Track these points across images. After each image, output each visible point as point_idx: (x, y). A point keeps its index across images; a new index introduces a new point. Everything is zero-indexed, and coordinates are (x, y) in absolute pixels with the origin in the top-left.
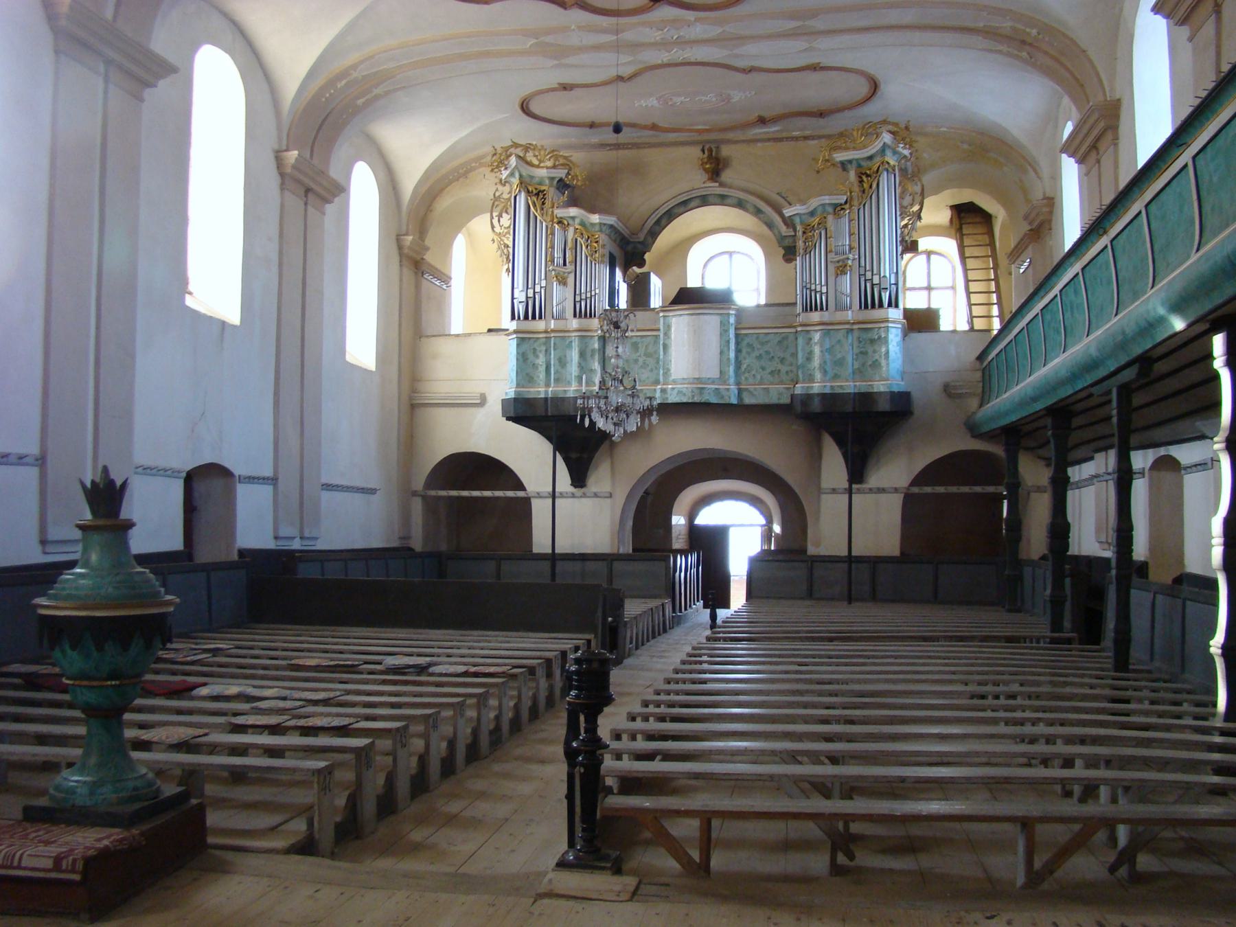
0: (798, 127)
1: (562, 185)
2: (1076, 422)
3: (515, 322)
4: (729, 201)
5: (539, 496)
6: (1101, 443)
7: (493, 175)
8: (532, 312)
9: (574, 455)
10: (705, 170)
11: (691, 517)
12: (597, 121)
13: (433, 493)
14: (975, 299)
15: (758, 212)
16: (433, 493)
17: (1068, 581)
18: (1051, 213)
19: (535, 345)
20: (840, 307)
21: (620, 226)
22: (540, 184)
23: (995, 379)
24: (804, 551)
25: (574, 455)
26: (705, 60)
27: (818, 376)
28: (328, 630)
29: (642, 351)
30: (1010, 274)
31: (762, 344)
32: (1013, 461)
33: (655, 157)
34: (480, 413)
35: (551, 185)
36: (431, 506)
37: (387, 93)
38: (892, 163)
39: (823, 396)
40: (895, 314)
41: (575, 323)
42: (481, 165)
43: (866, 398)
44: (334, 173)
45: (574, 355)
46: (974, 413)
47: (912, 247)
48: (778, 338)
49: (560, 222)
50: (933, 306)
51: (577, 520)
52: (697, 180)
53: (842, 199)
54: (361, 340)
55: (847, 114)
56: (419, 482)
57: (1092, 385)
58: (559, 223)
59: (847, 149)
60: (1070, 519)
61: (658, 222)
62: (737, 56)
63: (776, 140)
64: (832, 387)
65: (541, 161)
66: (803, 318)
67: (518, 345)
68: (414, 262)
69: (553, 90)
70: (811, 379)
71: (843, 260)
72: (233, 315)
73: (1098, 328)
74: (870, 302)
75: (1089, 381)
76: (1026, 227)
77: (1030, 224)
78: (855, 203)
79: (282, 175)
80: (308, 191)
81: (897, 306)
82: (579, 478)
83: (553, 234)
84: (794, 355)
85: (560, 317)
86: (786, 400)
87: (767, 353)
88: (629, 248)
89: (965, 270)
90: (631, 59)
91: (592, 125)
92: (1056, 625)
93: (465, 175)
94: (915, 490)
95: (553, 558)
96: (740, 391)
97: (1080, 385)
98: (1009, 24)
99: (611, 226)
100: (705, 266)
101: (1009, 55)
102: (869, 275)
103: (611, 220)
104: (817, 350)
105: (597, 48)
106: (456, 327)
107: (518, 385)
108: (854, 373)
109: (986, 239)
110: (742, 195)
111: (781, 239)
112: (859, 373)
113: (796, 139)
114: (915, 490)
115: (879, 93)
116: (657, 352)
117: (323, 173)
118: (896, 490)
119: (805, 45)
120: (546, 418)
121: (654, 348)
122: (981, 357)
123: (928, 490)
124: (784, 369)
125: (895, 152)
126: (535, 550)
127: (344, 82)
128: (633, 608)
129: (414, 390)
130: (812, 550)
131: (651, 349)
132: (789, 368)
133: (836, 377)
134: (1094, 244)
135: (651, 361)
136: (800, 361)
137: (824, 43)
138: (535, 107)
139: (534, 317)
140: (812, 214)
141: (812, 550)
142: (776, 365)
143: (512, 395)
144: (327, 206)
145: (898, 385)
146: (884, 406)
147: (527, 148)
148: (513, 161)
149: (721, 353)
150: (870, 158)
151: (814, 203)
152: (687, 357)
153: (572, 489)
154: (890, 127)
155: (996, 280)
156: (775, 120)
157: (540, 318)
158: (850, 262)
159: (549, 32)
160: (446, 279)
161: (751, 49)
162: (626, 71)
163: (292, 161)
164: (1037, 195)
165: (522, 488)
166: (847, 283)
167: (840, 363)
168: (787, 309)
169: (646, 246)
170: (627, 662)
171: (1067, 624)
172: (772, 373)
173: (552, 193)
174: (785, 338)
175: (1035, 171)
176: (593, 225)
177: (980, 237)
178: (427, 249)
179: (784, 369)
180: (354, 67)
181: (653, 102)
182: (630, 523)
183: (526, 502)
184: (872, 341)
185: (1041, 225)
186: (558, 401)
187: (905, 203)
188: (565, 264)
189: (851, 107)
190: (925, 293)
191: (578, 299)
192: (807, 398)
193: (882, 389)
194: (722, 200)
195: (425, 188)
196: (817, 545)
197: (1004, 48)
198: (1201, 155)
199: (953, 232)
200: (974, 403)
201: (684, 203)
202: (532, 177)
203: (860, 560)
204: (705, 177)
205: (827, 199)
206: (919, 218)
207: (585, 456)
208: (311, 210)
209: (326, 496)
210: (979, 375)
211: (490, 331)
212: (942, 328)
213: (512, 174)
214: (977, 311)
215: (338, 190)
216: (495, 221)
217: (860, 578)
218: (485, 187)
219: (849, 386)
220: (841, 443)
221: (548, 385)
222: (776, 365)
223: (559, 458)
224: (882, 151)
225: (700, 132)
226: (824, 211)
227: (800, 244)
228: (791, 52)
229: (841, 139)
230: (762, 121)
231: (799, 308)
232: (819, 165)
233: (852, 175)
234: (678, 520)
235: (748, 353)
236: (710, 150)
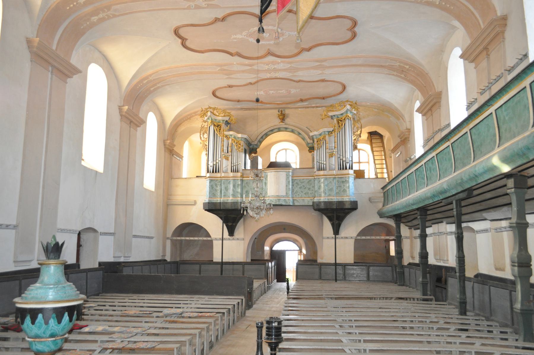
0: (314, 103)
1: (227, 123)
2: (429, 212)
4: (288, 130)
5: (216, 239)
6: (434, 221)
7: (201, 119)
8: (216, 170)
9: (230, 224)
10: (280, 118)
11: (271, 248)
12: (240, 99)
13: (175, 238)
14: (378, 166)
15: (299, 134)
16: (175, 238)
17: (428, 275)
18: (409, 134)
19: (216, 182)
21: (248, 138)
23: (390, 196)
24: (316, 261)
25: (230, 224)
26: (283, 77)
27: (323, 195)
28: (135, 296)
30: (391, 157)
32: (398, 227)
34: (194, 208)
36: (174, 243)
37: (162, 86)
38: (350, 116)
39: (325, 202)
40: (351, 172)
41: (231, 174)
42: (196, 115)
43: (341, 203)
44: (141, 115)
45: (231, 186)
46: (381, 209)
47: (355, 148)
49: (226, 137)
50: (361, 169)
51: (231, 249)
52: (276, 122)
53: (331, 129)
54: (150, 180)
55: (333, 98)
56: (169, 234)
57: (442, 200)
59: (333, 111)
60: (428, 251)
61: (262, 137)
62: (296, 76)
63: (306, 108)
67: (210, 182)
68: (170, 150)
69: (225, 87)
70: (320, 196)
72: (101, 169)
73: (444, 177)
74: (343, 167)
75: (441, 198)
76: (399, 140)
77: (401, 139)
78: (336, 131)
79: (121, 115)
80: (131, 122)
81: (352, 169)
82: (231, 233)
83: (223, 141)
84: (314, 187)
85: (226, 172)
87: (304, 186)
88: (251, 147)
89: (374, 156)
90: (255, 76)
91: (238, 101)
92: (424, 293)
93: (190, 118)
94: (359, 238)
95: (222, 263)
96: (293, 200)
97: (436, 199)
98: (399, 64)
99: (245, 139)
100: (277, 154)
101: (397, 76)
102: (341, 157)
103: (245, 136)
104: (322, 185)
105: (243, 71)
106: (185, 175)
107: (210, 198)
108: (336, 193)
109: (381, 144)
110: (293, 128)
111: (308, 144)
112: (337, 194)
113: (314, 107)
114: (359, 238)
115: (346, 90)
117: (137, 115)
119: (320, 72)
120: (220, 210)
122: (383, 188)
123: (364, 238)
125: (351, 112)
126: (214, 261)
127: (146, 81)
128: (256, 284)
129: (169, 199)
130: (319, 261)
133: (330, 195)
134: (442, 145)
136: (316, 189)
137: (327, 71)
138: (217, 94)
139: (216, 172)
140: (320, 135)
141: (319, 261)
142: (306, 190)
143: (207, 201)
144: (138, 128)
145: (353, 198)
146: (348, 206)
147: (214, 109)
148: (209, 113)
149: (286, 186)
150: (342, 114)
151: (321, 131)
152: (275, 186)
153: (229, 237)
154: (349, 103)
155: (385, 159)
156: (306, 100)
159: (225, 65)
160: (181, 157)
161: (300, 73)
162: (253, 81)
163: (126, 110)
164: (403, 128)
165: (210, 237)
166: (334, 161)
167: (331, 190)
169: (258, 146)
170: (254, 306)
171: (429, 293)
172: (305, 194)
173: (223, 126)
174: (310, 180)
175: (403, 119)
176: (238, 138)
177: (378, 144)
178: (175, 146)
179: (310, 192)
180: (150, 75)
181: (262, 93)
182: (250, 250)
183: (211, 241)
184: (343, 182)
185: (405, 139)
186: (225, 203)
189: (334, 96)
190: (358, 164)
193: (347, 200)
194: (286, 129)
195: (175, 123)
196: (322, 259)
197: (395, 73)
198: (499, 109)
199: (369, 142)
200: (380, 205)
201: (272, 130)
202: (216, 120)
203: (340, 265)
204: (280, 121)
205: (326, 129)
206: (360, 136)
208: (132, 129)
209: (134, 240)
210: (382, 194)
211: (197, 177)
212: (366, 176)
213: (208, 119)
214: (378, 171)
215: (142, 122)
216: (202, 136)
217: (338, 272)
218: (198, 123)
219: (335, 199)
220: (330, 219)
221: (221, 198)
223: (224, 225)
224: (347, 112)
225: (277, 104)
226: (325, 134)
227: (316, 146)
228: (315, 75)
229: (331, 107)
230: (302, 100)
231: (315, 170)
232: (324, 117)
233: (335, 120)
234: (267, 248)
236: (282, 111)
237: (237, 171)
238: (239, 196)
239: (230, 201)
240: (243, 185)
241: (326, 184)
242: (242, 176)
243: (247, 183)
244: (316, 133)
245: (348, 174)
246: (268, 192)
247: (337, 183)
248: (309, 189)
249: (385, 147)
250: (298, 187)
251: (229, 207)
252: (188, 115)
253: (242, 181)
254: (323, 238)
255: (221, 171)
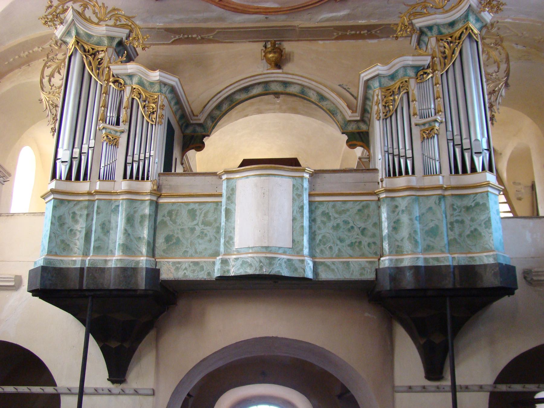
3: (54, 181)
8: (77, 173)
9: (114, 344)
10: (268, 61)
19: (76, 209)
20: (428, 172)
22: (98, 44)
25: (114, 344)
27: (407, 246)
29: (200, 219)
31: (340, 213)
33: (216, 51)
35: (110, 46)
38: (476, 31)
39: (416, 269)
41: (124, 185)
43: (469, 271)
48: (358, 207)
53: (426, 60)
58: (114, 82)
61: (219, 107)
64: (426, 260)
65: (100, 20)
66: (388, 183)
67: (55, 207)
70: (397, 250)
71: (429, 122)
82: (118, 372)
84: (378, 225)
86: (370, 276)
87: (346, 222)
88: (189, 131)
94: (503, 388)
99: (173, 90)
104: (405, 219)
107: (50, 253)
108: (450, 243)
114: (503, 388)
116: (217, 220)
118: (481, 388)
120: (81, 293)
121: (213, 212)
124: (365, 241)
131: (211, 218)
132: (371, 240)
133: (428, 249)
135: (210, 231)
136: (385, 232)
139: (78, 178)
140: (392, 77)
146: (490, 280)
148: (69, 15)
149: (294, 219)
150: (452, 24)
151: (398, 63)
153: (109, 385)
157: (85, 179)
158: (437, 125)
168: (367, 176)
172: (351, 245)
174: (366, 206)
176: (152, 84)
179: (365, 241)
183: (55, 399)
184: (468, 209)
186: (97, 271)
187: (491, 70)
188: (118, 123)
191: (129, 160)
192: (397, 272)
202: (90, 36)
205: (410, 60)
207: (127, 345)
213: (68, 33)
219: (448, 258)
221: (86, 253)
222: (355, 235)
223: (94, 348)
224: (466, 17)
225: (267, 12)
226: (405, 75)
231: (381, 174)
235: (324, 223)
236: (274, 45)
237: (142, 177)
238: (144, 250)
239: (112, 265)
240: (159, 219)
241: (416, 212)
242: (158, 192)
243: (170, 213)
244: (380, 69)
245: (488, 184)
246: (237, 239)
247: (449, 212)
248: (363, 231)
249: (504, 176)
250: (330, 224)
251: (111, 283)
252: (23, 46)
253: (156, 206)
254: (394, 390)
255: (95, 175)
